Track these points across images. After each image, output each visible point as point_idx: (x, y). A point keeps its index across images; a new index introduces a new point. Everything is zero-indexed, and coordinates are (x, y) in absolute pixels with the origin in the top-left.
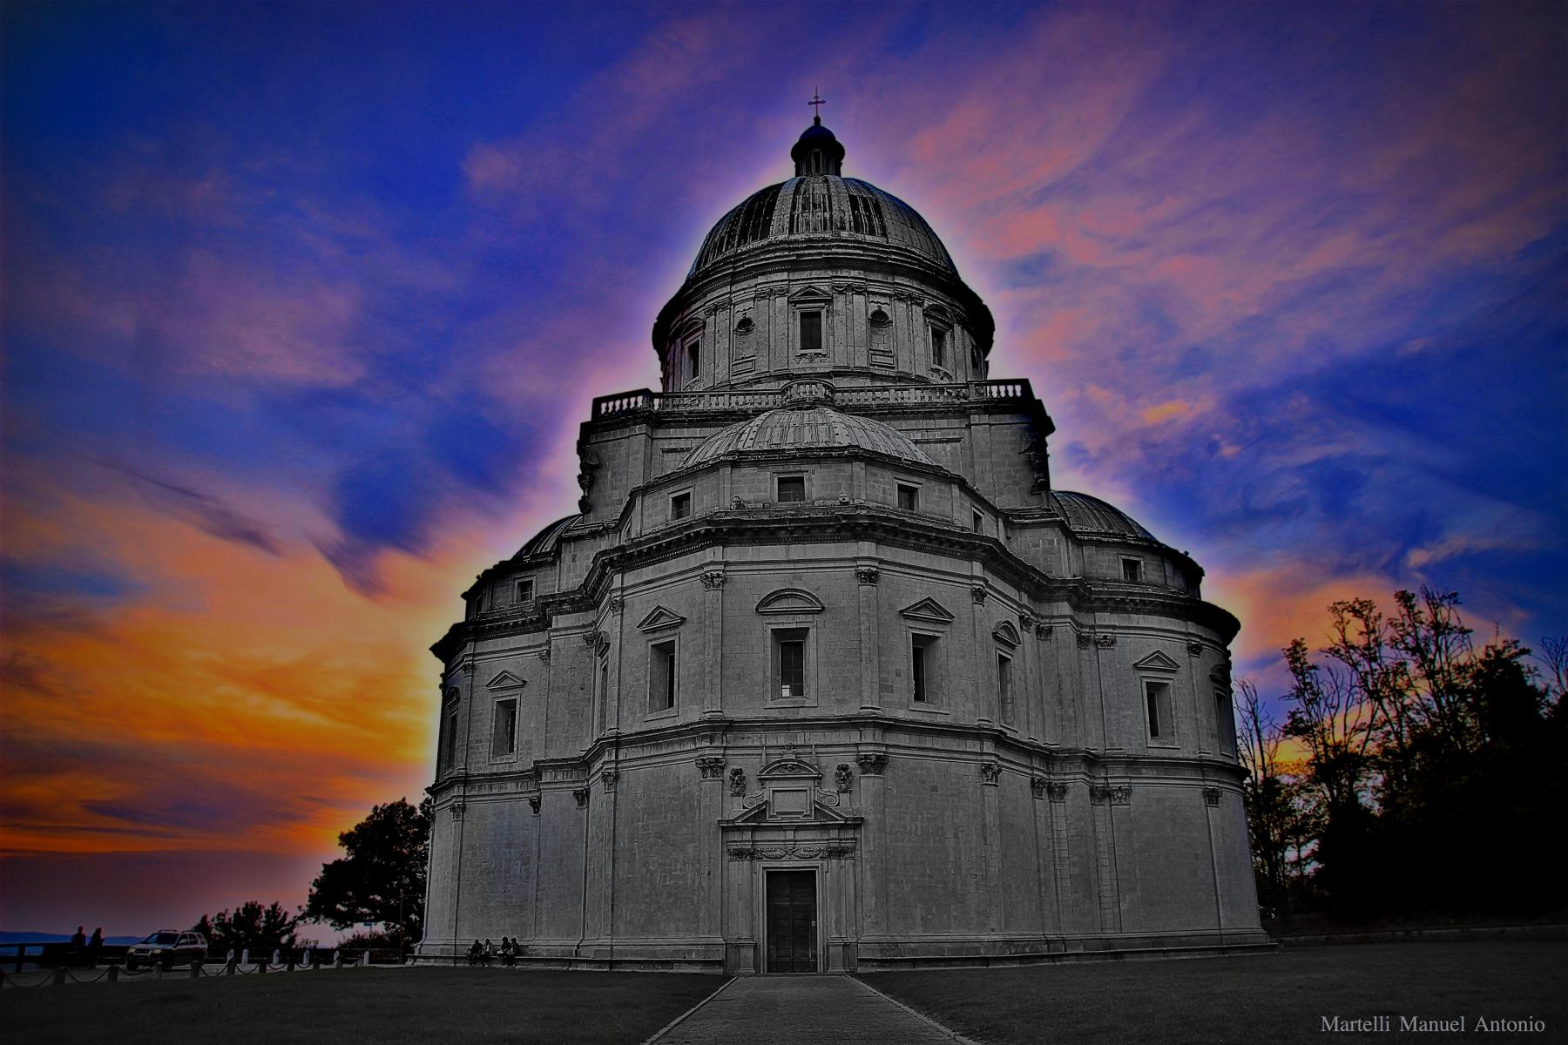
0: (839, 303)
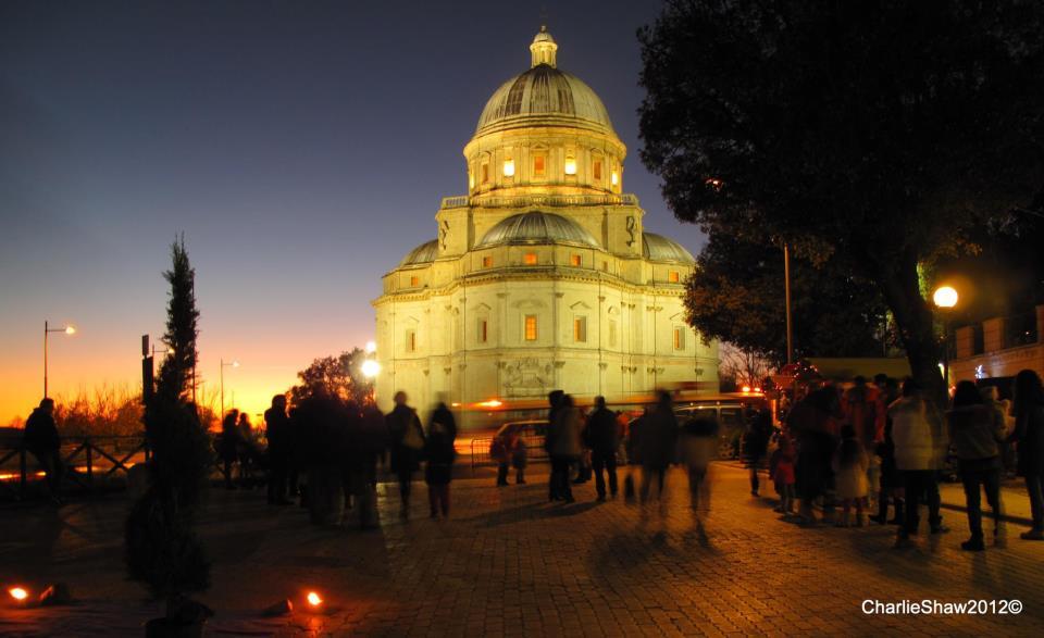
0: (552, 153)
